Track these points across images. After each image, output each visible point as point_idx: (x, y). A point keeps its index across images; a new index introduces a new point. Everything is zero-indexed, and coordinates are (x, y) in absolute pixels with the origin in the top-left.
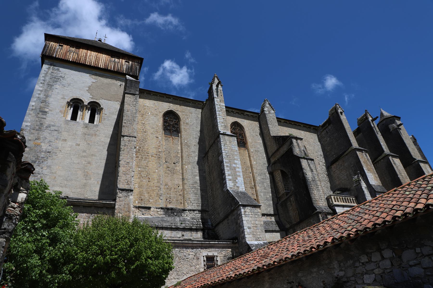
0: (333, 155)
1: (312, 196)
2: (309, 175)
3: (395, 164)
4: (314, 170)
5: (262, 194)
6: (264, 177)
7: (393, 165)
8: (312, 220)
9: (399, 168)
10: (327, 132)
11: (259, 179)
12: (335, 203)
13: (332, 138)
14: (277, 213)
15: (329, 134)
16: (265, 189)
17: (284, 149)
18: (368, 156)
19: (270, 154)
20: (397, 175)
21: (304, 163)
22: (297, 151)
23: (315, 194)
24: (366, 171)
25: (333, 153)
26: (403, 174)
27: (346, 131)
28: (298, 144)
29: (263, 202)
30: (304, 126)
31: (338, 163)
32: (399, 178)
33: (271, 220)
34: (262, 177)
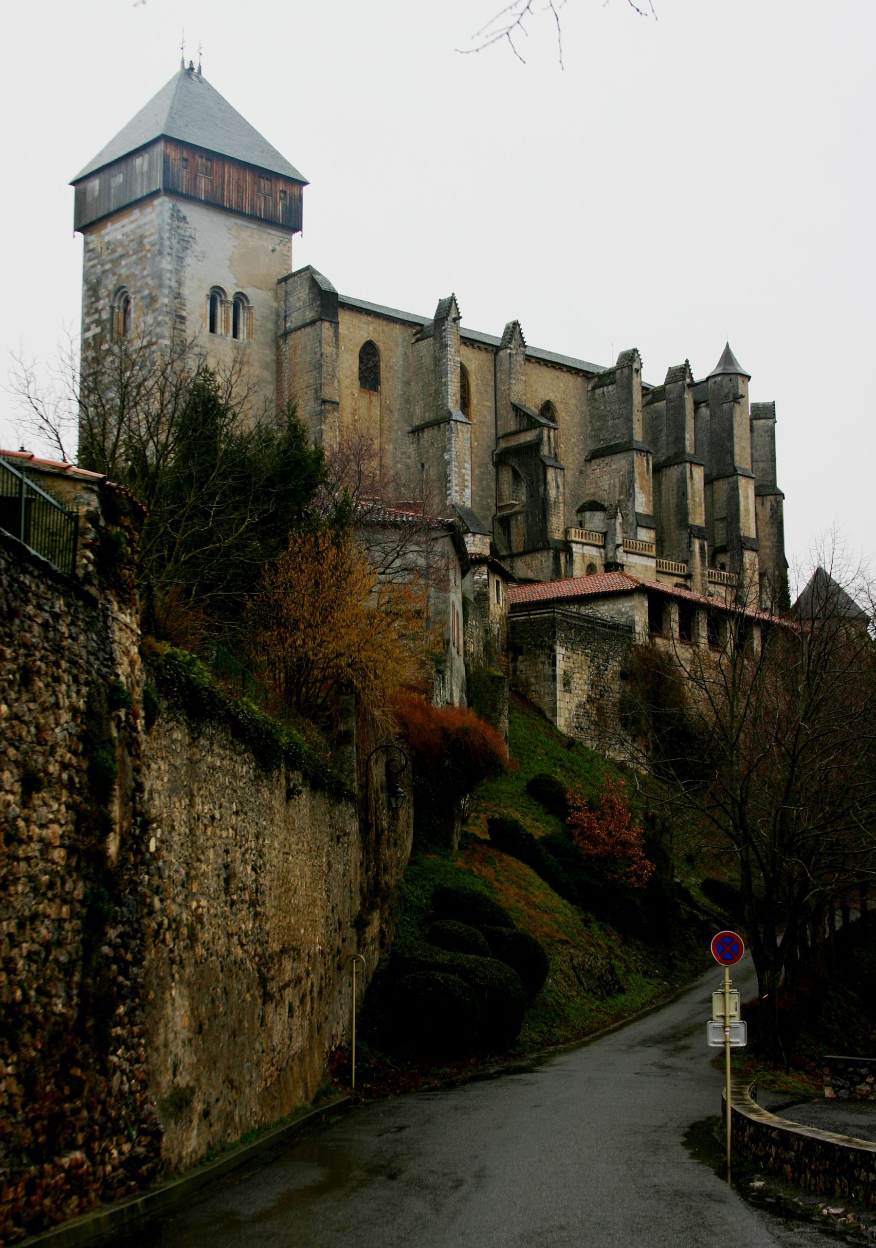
2: (552, 493)
3: (692, 478)
4: (561, 487)
7: (688, 480)
16: (483, 490)
17: (529, 437)
19: (501, 433)
20: (687, 499)
21: (551, 474)
22: (545, 451)
24: (637, 490)
26: (697, 499)
28: (549, 437)
32: (686, 505)
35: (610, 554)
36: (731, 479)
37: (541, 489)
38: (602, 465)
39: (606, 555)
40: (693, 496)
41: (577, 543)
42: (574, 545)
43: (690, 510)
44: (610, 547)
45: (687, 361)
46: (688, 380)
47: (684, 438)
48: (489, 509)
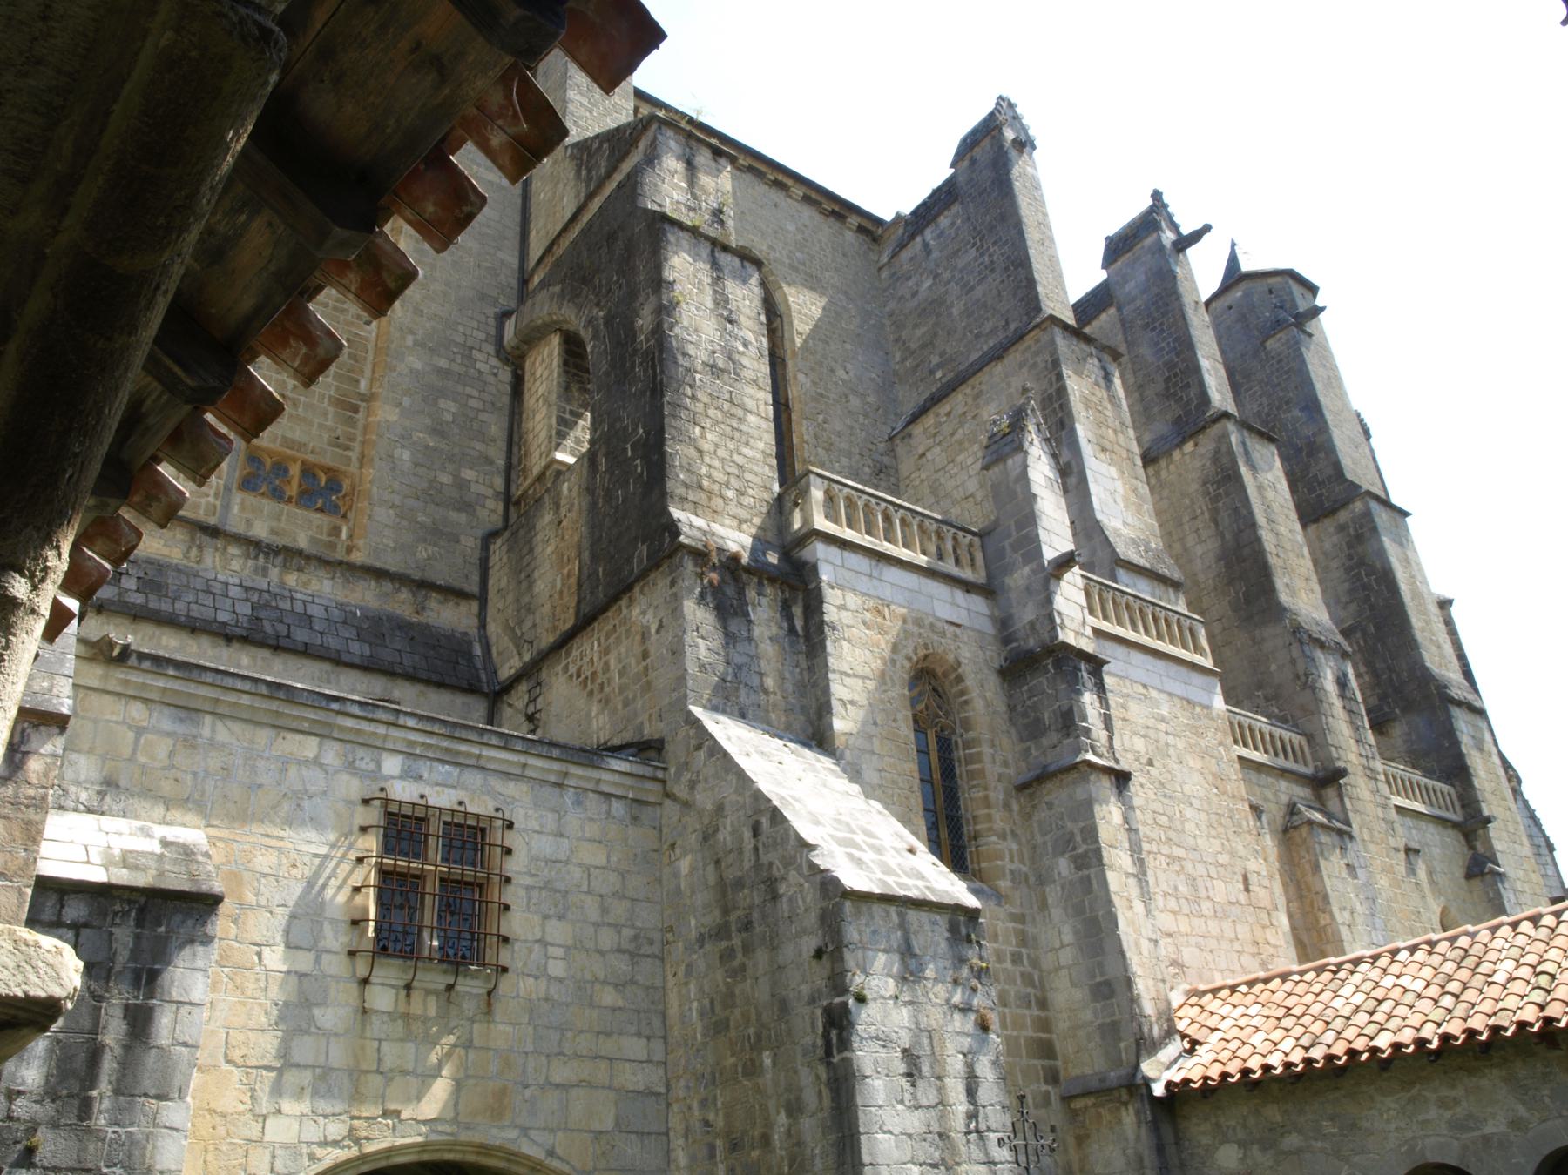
0: (932, 372)
1: (678, 451)
5: (406, 455)
6: (456, 368)
8: (636, 611)
9: (1270, 494)
10: (926, 245)
11: (418, 365)
12: (821, 523)
13: (947, 275)
14: (474, 588)
15: (935, 254)
16: (438, 431)
18: (1117, 382)
23: (706, 447)
25: (935, 360)
26: (1282, 529)
27: (1021, 233)
29: (397, 500)
30: (806, 199)
31: (947, 408)
32: (1258, 540)
33: (415, 619)
34: (443, 363)
35: (1026, 615)
36: (1343, 516)
37: (644, 322)
38: (947, 429)
39: (1004, 625)
40: (1270, 521)
41: (844, 544)
42: (821, 551)
43: (1272, 560)
44: (1019, 577)
45: (1157, 196)
46: (1168, 237)
47: (1197, 369)
48: (466, 507)
